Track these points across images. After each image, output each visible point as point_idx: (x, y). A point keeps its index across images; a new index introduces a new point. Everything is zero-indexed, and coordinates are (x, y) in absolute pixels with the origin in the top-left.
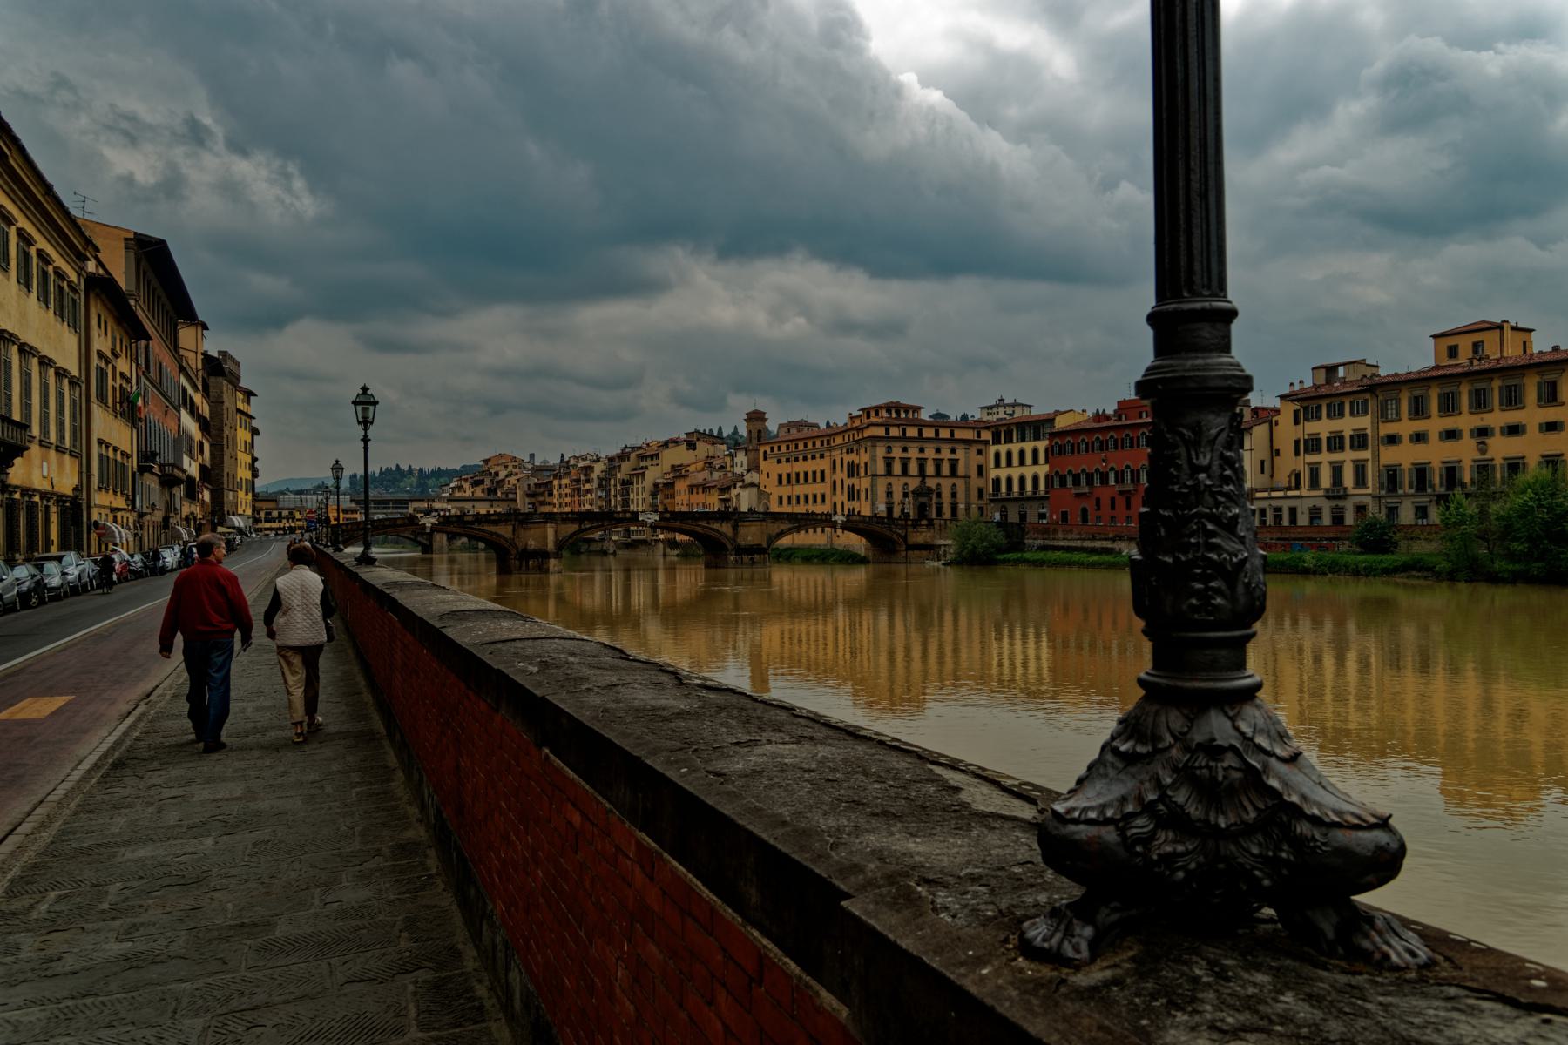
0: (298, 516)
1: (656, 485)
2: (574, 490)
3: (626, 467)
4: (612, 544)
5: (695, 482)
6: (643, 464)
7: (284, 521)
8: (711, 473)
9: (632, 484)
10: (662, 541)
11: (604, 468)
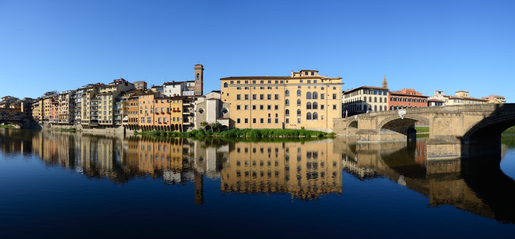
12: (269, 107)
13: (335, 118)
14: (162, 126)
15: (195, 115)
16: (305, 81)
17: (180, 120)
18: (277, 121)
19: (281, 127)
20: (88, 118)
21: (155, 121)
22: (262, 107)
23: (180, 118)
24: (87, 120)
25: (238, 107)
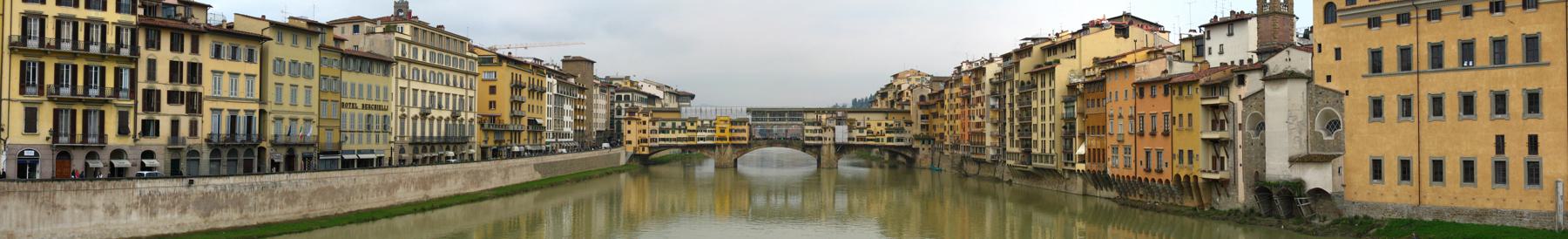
0: (689, 127)
1: (1072, 87)
2: (964, 98)
3: (1027, 64)
4: (1007, 169)
5: (1145, 77)
6: (1049, 59)
7: (677, 132)
8: (1171, 64)
9: (1036, 86)
10: (1082, 174)
11: (999, 69)
14: (1153, 180)
15: (1239, 141)
17: (1194, 160)
20: (1017, 146)
21: (1139, 163)
23: (1195, 153)
24: (1016, 150)
25: (1377, 107)
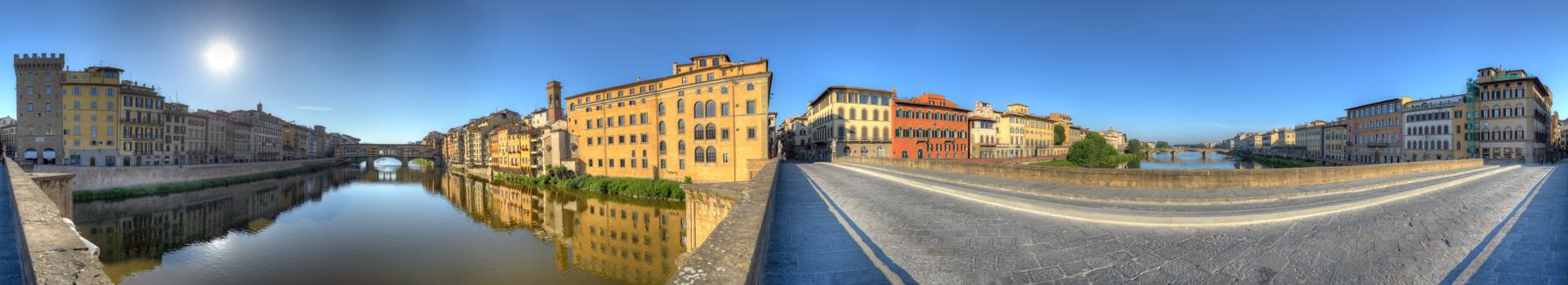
12: (633, 139)
13: (752, 160)
16: (691, 79)
18: (645, 164)
19: (651, 176)
22: (622, 139)
